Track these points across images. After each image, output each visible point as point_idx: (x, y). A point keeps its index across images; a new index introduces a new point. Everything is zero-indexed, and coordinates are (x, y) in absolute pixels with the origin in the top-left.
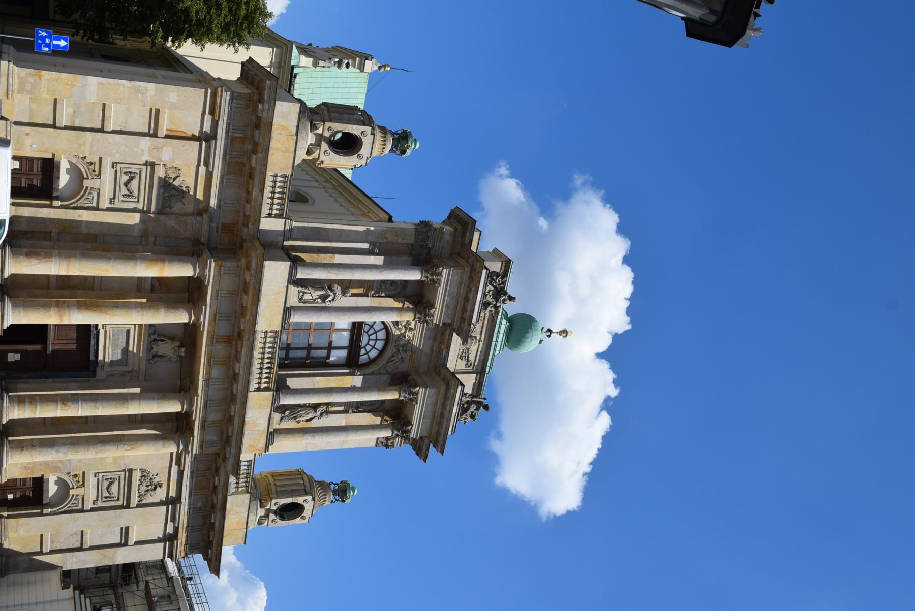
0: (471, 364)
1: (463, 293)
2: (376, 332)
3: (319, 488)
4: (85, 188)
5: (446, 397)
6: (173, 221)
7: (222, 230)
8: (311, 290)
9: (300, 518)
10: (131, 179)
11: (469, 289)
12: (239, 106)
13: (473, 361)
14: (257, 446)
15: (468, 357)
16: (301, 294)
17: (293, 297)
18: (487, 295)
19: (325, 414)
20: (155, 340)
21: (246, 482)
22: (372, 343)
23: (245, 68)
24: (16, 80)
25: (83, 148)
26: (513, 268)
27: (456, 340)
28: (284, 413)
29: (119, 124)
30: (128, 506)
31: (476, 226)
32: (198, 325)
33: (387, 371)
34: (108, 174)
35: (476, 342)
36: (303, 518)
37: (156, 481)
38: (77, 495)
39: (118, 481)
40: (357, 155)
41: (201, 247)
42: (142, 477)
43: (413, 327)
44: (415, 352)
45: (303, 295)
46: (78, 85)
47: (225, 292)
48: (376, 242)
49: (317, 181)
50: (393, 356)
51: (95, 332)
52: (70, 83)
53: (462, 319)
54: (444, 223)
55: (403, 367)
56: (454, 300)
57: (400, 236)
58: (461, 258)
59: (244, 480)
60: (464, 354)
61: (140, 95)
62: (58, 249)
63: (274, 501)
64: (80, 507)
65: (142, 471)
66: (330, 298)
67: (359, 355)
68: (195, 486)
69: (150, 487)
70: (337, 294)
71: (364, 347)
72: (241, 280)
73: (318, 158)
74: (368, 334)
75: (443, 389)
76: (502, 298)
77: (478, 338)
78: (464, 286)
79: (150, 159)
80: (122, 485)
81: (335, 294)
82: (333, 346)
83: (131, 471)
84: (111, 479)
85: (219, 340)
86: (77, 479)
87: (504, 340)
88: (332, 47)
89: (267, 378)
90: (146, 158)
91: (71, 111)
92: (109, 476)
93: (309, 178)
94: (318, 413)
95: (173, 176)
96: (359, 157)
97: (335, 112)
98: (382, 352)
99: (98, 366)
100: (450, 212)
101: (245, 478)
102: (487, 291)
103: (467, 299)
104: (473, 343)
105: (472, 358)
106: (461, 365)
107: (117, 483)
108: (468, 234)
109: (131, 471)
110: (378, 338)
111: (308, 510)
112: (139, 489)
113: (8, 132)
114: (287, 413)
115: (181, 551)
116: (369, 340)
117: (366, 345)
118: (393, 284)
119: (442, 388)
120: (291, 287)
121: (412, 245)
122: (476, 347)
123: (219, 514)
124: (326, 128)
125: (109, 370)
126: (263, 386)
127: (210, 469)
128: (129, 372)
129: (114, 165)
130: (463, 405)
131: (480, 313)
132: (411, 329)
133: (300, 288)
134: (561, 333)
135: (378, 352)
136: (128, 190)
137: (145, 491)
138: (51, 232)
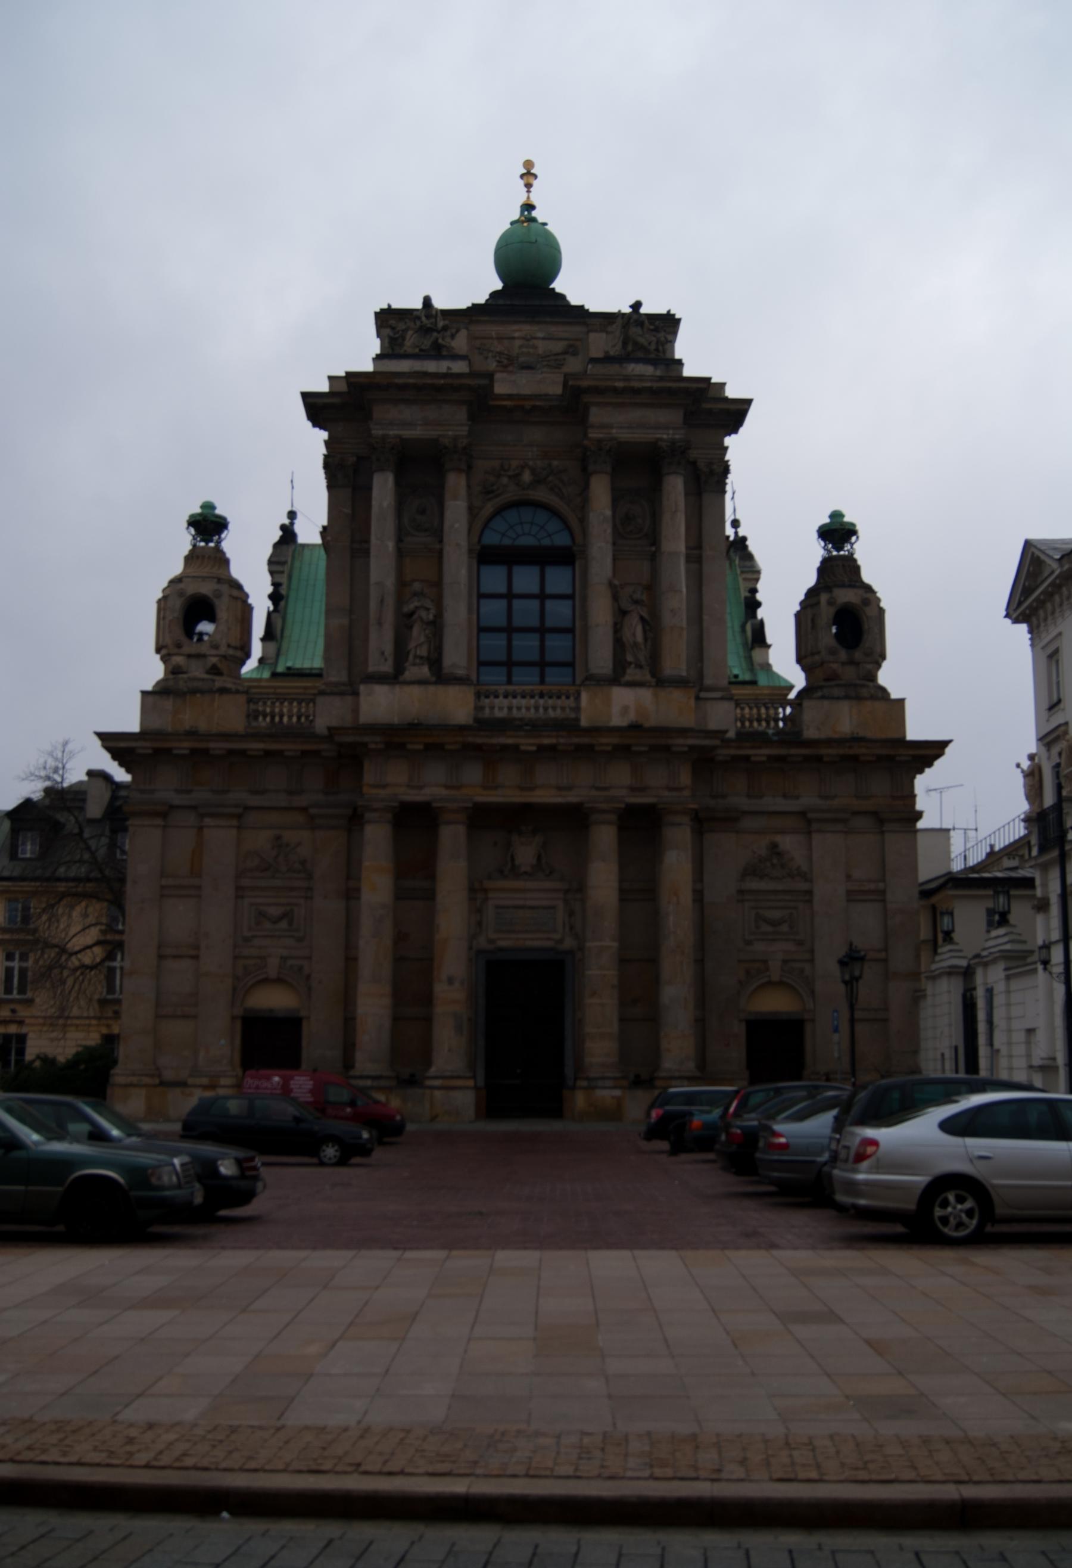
8: (412, 645)
13: (565, 343)
16: (418, 661)
18: (421, 350)
28: (630, 663)
30: (810, 893)
66: (423, 614)
69: (775, 861)
70: (416, 604)
81: (417, 608)
83: (741, 892)
101: (767, 709)
105: (559, 346)
109: (741, 892)
114: (630, 658)
123: (824, 751)
124: (176, 651)
133: (407, 664)
134: (528, 186)
136: (280, 918)
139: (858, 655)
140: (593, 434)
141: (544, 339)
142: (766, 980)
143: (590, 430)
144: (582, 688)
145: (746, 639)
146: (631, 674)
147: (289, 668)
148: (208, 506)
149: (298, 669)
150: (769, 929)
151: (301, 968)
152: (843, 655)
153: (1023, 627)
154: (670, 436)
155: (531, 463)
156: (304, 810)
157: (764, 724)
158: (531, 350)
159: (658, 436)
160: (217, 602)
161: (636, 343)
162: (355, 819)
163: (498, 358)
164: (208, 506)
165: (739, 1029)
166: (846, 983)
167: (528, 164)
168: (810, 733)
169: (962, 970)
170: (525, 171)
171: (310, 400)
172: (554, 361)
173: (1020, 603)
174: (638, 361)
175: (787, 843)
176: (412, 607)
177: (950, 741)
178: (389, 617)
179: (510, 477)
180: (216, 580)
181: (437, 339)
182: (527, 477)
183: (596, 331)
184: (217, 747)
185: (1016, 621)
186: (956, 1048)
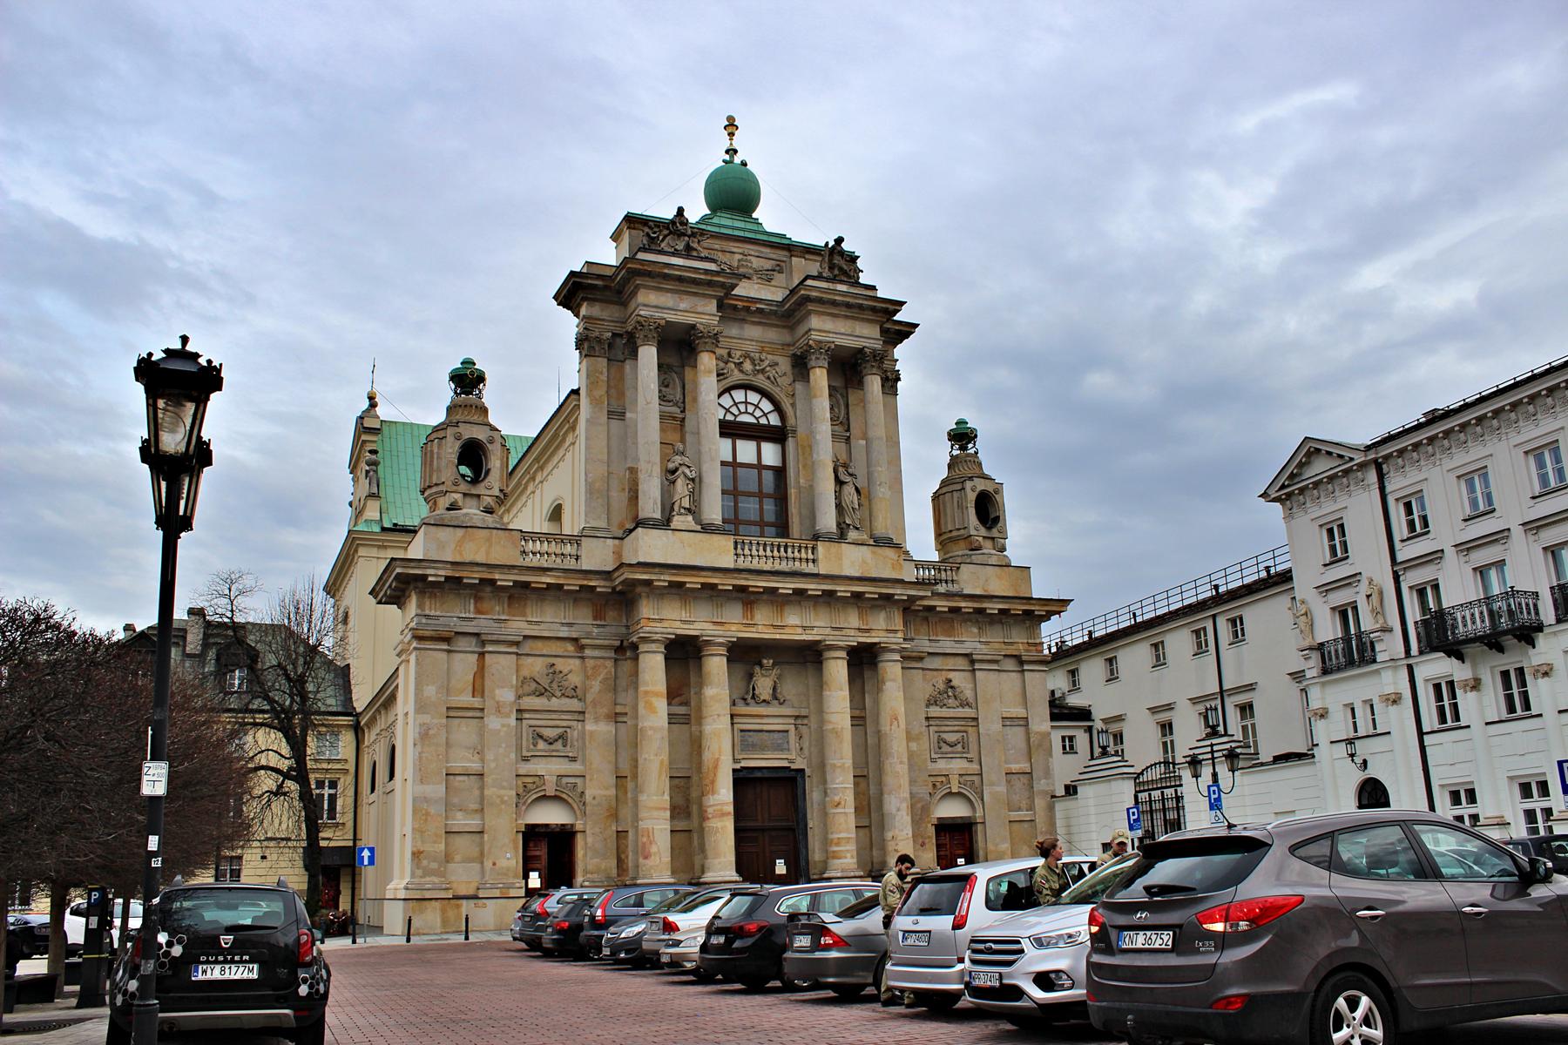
0: (778, 265)
1: (673, 285)
2: (736, 404)
3: (957, 471)
4: (558, 793)
5: (820, 301)
6: (593, 683)
9: (996, 496)
10: (541, 737)
11: (666, 277)
12: (433, 606)
15: (768, 270)
16: (682, 511)
17: (688, 522)
18: (675, 250)
19: (850, 470)
20: (754, 694)
21: (945, 570)
22: (751, 409)
23: (383, 600)
24: (428, 879)
25: (506, 798)
26: (638, 209)
27: (743, 289)
28: (849, 525)
30: (976, 719)
31: (578, 270)
32: (730, 644)
34: (538, 767)
35: (746, 260)
36: (997, 491)
37: (942, 686)
38: (960, 783)
39: (941, 734)
41: (625, 643)
42: (937, 705)
43: (727, 351)
44: (762, 347)
45: (685, 509)
47: (683, 612)
48: (608, 411)
49: (534, 492)
50: (769, 378)
52: (424, 818)
53: (710, 284)
54: (577, 315)
55: (785, 365)
56: (685, 297)
57: (598, 377)
58: (624, 289)
59: (943, 572)
60: (763, 276)
61: (431, 732)
62: (637, 822)
63: (973, 532)
64: (975, 778)
65: (927, 706)
67: (769, 426)
68: (950, 636)
69: (950, 694)
70: (681, 462)
72: (665, 592)
73: (497, 497)
75: (811, 307)
76: (680, 228)
77: (740, 257)
78: (663, 283)
79: (514, 716)
80: (947, 729)
81: (680, 465)
82: (756, 462)
83: (927, 718)
84: (939, 743)
85: (749, 617)
86: (937, 784)
87: (742, 219)
88: (351, 473)
89: (799, 551)
90: (512, 721)
92: (934, 745)
93: (530, 502)
94: (848, 479)
95: (534, 685)
97: (431, 477)
98: (764, 394)
100: (561, 307)
102: (670, 250)
103: (680, 279)
105: (768, 265)
106: (780, 279)
108: (589, 282)
109: (927, 718)
110: (744, 400)
111: (986, 486)
112: (954, 708)
113: (493, 886)
116: (746, 412)
118: (666, 383)
119: (810, 308)
120: (673, 525)
121: (608, 360)
122: (753, 259)
124: (455, 488)
125: (794, 753)
126: (810, 556)
127: (926, 619)
128: (796, 729)
129: (526, 759)
130: (835, 276)
131: (702, 258)
132: (729, 355)
134: (731, 135)
135: (764, 399)
136: (557, 740)
137: (956, 699)
138: (618, 832)
139: (995, 533)
140: (815, 336)
141: (758, 257)
142: (949, 790)
146: (852, 535)
147: (395, 525)
148: (468, 363)
150: (950, 749)
151: (575, 785)
152: (983, 531)
154: (872, 345)
155: (752, 354)
156: (576, 640)
158: (749, 264)
159: (864, 344)
161: (841, 269)
162: (627, 650)
164: (468, 363)
165: (931, 831)
167: (731, 120)
170: (727, 123)
173: (1283, 487)
174: (841, 282)
175: (959, 679)
176: (676, 464)
178: (657, 470)
179: (735, 363)
182: (748, 366)
183: (797, 257)
184: (504, 579)
185: (1274, 500)
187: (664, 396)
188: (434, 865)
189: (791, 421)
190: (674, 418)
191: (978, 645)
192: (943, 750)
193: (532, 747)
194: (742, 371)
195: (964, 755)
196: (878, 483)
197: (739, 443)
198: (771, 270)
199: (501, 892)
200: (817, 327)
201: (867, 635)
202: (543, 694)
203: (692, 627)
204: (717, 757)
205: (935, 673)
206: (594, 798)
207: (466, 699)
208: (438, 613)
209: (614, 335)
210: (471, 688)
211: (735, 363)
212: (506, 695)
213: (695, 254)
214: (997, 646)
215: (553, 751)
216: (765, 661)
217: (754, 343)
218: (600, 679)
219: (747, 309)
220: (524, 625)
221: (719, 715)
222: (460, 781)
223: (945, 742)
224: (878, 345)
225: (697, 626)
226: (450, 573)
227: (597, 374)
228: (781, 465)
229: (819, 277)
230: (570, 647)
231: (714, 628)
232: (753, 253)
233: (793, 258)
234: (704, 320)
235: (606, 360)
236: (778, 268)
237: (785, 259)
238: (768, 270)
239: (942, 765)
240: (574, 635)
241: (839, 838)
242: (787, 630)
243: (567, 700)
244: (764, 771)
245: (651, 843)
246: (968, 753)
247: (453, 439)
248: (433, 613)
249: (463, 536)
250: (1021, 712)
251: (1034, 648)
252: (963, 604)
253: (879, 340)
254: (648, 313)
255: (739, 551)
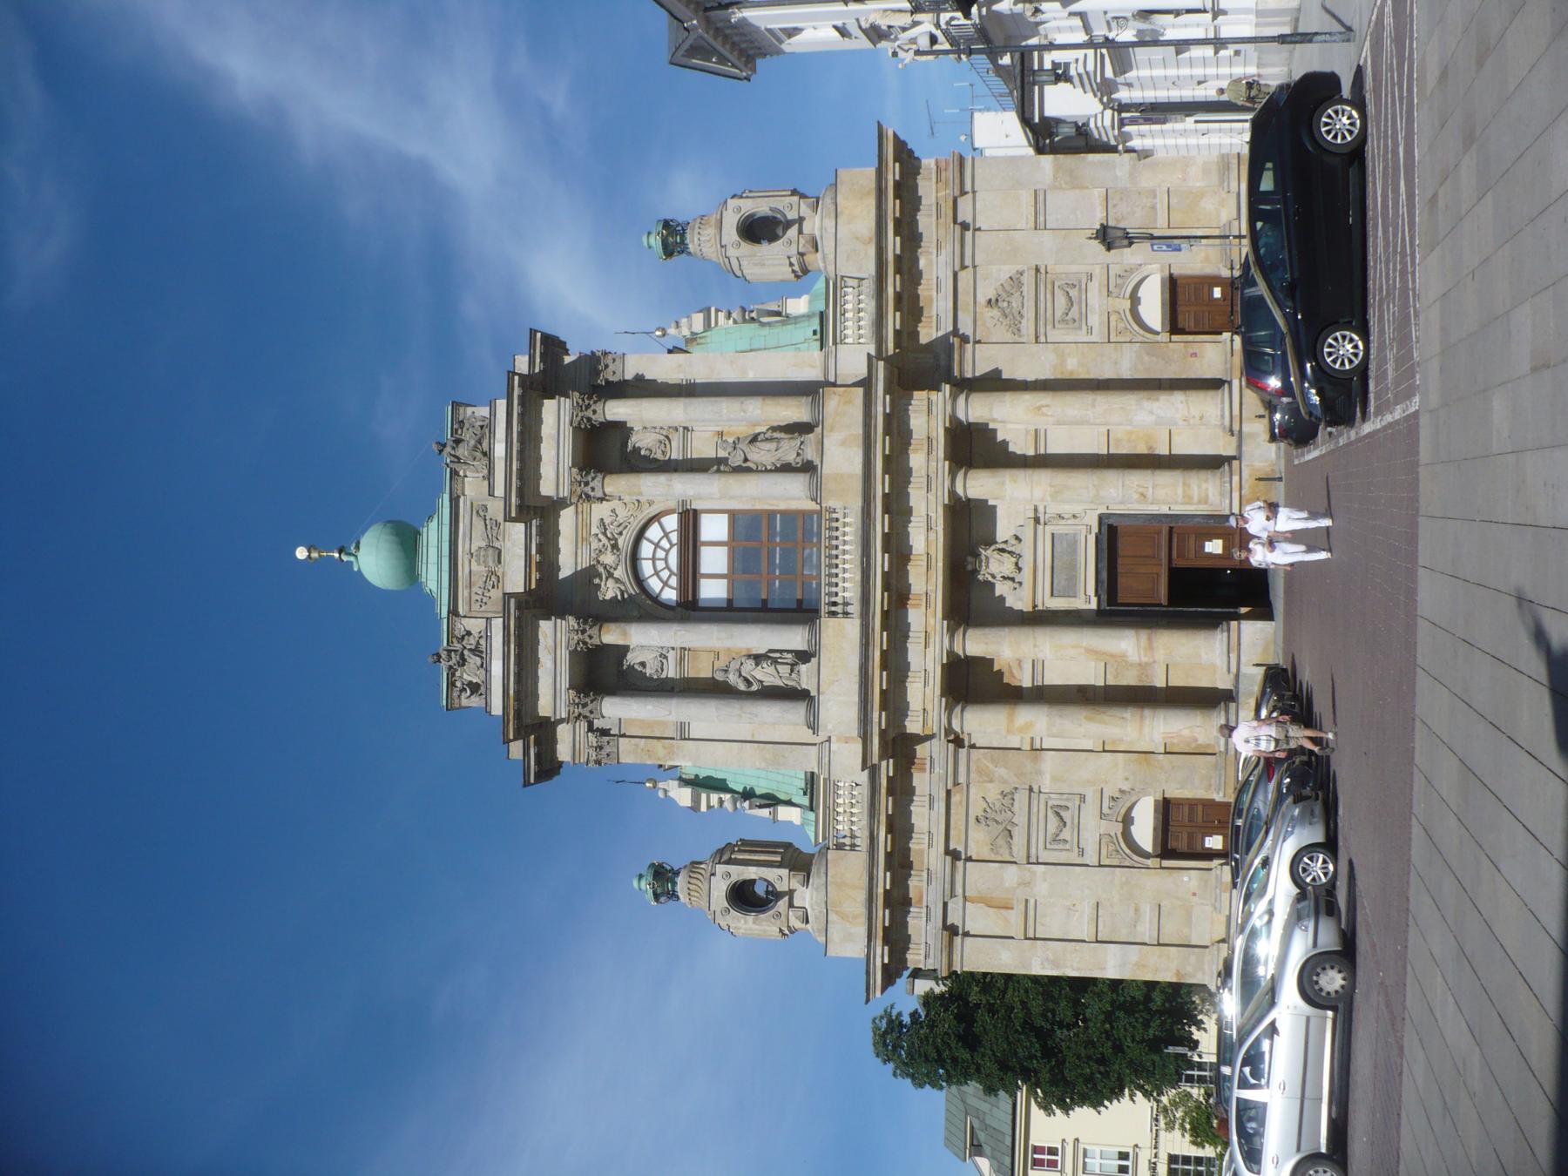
0: (478, 512)
7: (925, 764)
8: (780, 683)
14: (839, 402)
15: (486, 525)
18: (482, 666)
24: (1206, 967)
25: (1124, 879)
29: (1077, 913)
33: (625, 504)
34: (1090, 841)
37: (995, 312)
40: (731, 879)
46: (1131, 966)
50: (621, 533)
51: (1100, 592)
57: (642, 750)
61: (1051, 957)
68: (932, 300)
71: (672, 545)
74: (669, 569)
81: (740, 675)
91: (1139, 928)
96: (729, 875)
99: (1096, 534)
104: (484, 556)
105: (478, 524)
107: (1059, 314)
108: (532, 763)
110: (651, 561)
115: (946, 170)
116: (666, 559)
117: (670, 548)
124: (783, 918)
136: (1061, 818)
143: (561, 496)
144: (823, 505)
145: (777, 322)
146: (810, 454)
147: (805, 794)
149: (806, 784)
150: (1075, 308)
153: (759, 62)
156: (948, 793)
157: (861, 314)
158: (482, 553)
160: (734, 879)
161: (475, 448)
163: (490, 588)
166: (1130, 244)
168: (870, 269)
169: (1116, 113)
171: (532, 781)
172: (492, 528)
175: (986, 291)
177: (879, 122)
179: (607, 579)
180: (712, 877)
181: (470, 650)
184: (884, 880)
185: (754, 70)
186: (1196, 122)
187: (657, 671)
188: (1193, 959)
189: (672, 504)
190: (682, 659)
191: (942, 258)
192: (1077, 317)
193: (1068, 847)
194: (615, 569)
195: (1084, 286)
196: (742, 414)
197: (705, 568)
198: (485, 520)
199: (1225, 892)
200: (554, 487)
201: (935, 443)
202: (1010, 831)
203: (931, 675)
204: (1083, 651)
205: (978, 323)
206: (1127, 779)
207: (1015, 917)
208: (923, 946)
209: (591, 728)
210: (1003, 912)
211: (607, 579)
212: (1011, 874)
213: (482, 642)
214: (942, 232)
215: (1073, 823)
216: (970, 567)
217: (579, 551)
218: (991, 767)
219: (539, 564)
220: (933, 851)
221: (1035, 646)
222: (1104, 926)
223: (1067, 314)
224: (566, 403)
225: (930, 667)
226: (879, 941)
227: (639, 751)
228: (726, 515)
229: (490, 477)
230: (955, 799)
231: (932, 645)
232: (467, 546)
233: (466, 493)
234: (563, 639)
235: (621, 739)
236: (482, 514)
237: (468, 503)
238: (486, 525)
239: (1095, 320)
240: (943, 795)
241: (1184, 497)
242: (932, 553)
243: (1016, 804)
244: (1099, 566)
245: (1180, 736)
246: (1080, 282)
247: (728, 917)
248: (922, 952)
249: (837, 913)
250: (1026, 198)
251: (943, 174)
252: (890, 290)
253: (559, 402)
254: (563, 709)
255: (839, 609)
